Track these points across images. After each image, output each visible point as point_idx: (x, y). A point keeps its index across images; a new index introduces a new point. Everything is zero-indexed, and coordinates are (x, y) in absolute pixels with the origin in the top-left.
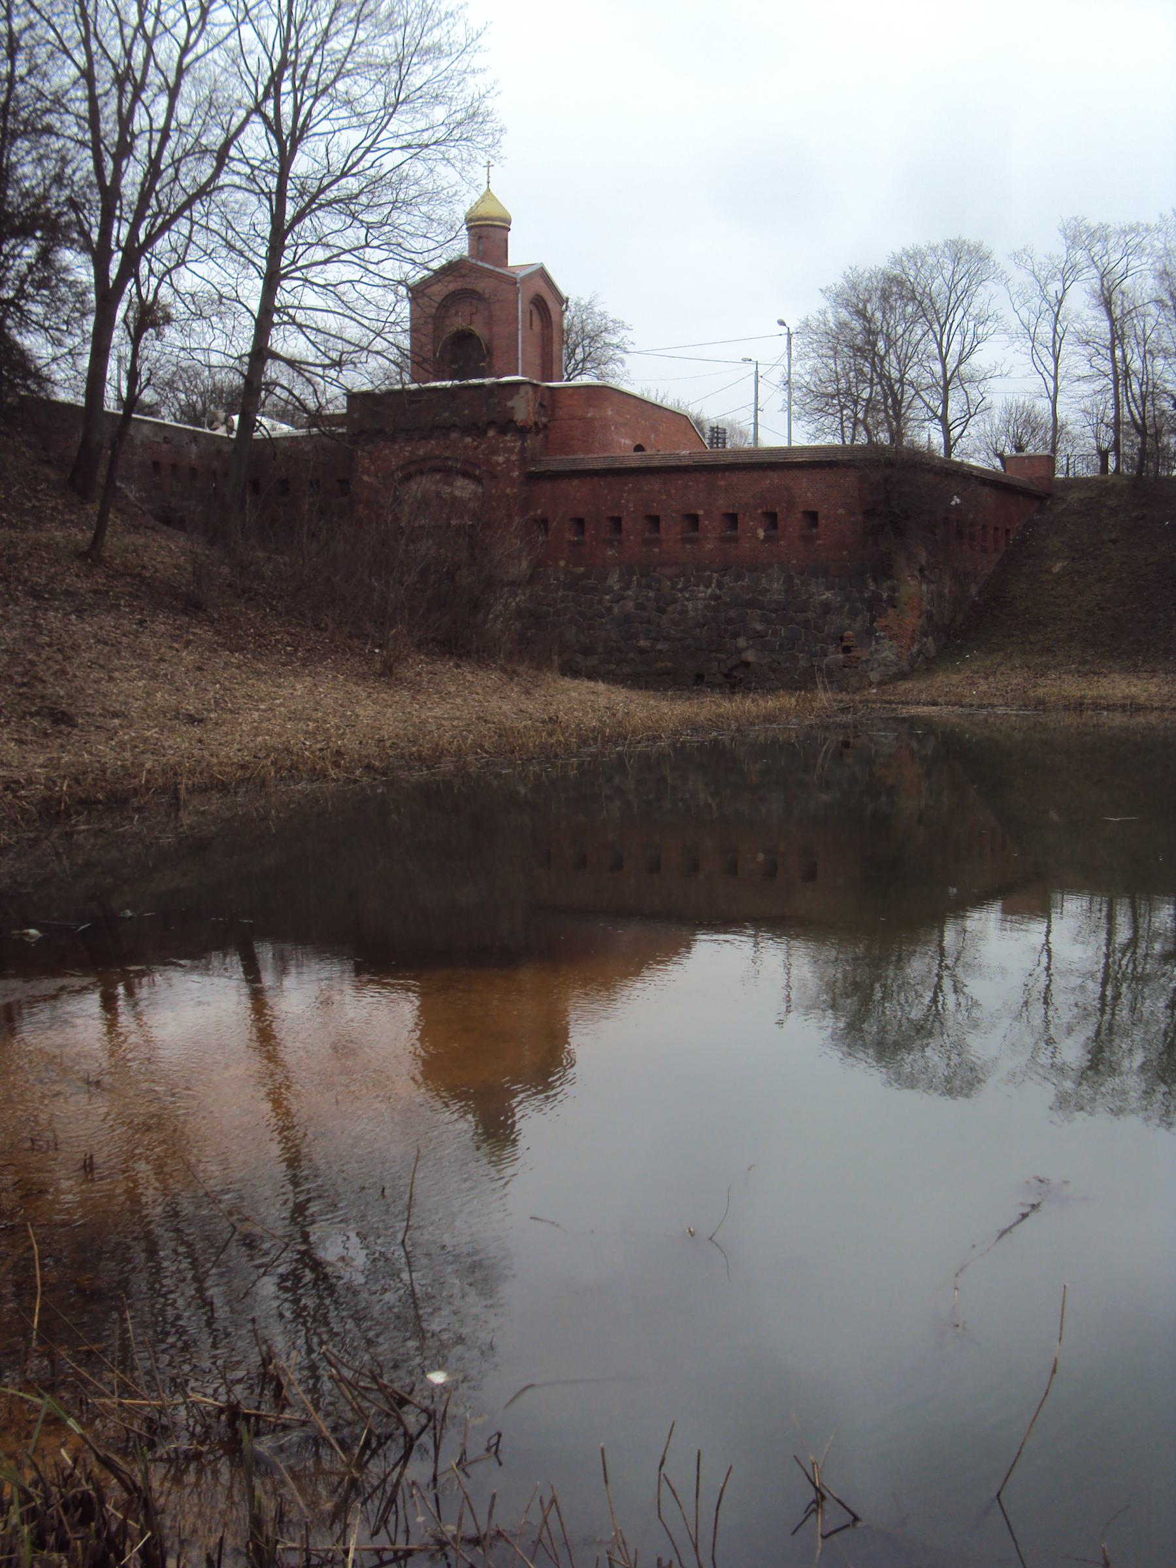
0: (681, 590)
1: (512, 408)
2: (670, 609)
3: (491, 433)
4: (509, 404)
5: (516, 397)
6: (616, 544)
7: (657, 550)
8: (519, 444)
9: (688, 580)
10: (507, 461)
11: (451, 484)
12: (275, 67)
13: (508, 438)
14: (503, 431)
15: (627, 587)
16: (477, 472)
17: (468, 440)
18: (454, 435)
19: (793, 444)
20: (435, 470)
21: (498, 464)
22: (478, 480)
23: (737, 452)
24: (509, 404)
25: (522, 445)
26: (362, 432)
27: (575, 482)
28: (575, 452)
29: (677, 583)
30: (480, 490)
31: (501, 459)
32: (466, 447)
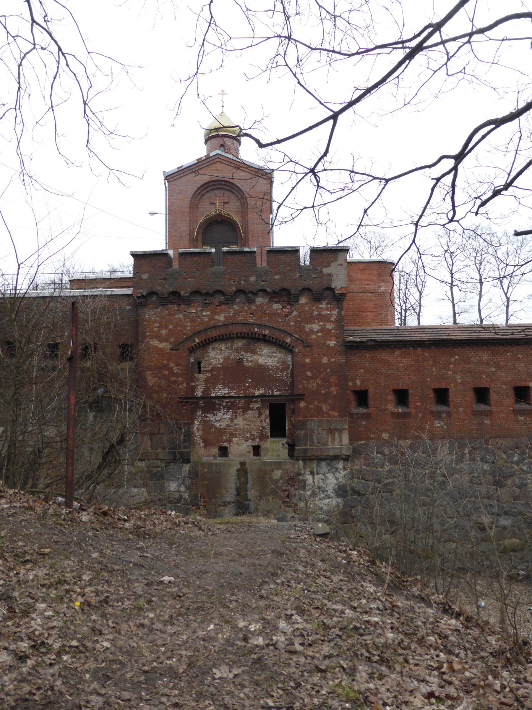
0: (517, 463)
1: (330, 275)
2: (509, 482)
3: (303, 300)
4: (326, 271)
5: (334, 264)
6: (444, 415)
7: (489, 422)
8: (335, 312)
9: (524, 453)
10: (323, 329)
11: (254, 353)
12: (508, 182)
13: (323, 305)
14: (317, 298)
15: (461, 459)
16: (288, 340)
17: (277, 306)
18: (259, 300)
19: (513, 321)
20: (241, 336)
21: (312, 331)
22: (288, 349)
23: (404, 329)
24: (326, 271)
25: (339, 313)
26: (152, 293)
27: (398, 352)
28: (369, 324)
29: (512, 455)
30: (289, 359)
31: (316, 327)
32: (275, 313)
